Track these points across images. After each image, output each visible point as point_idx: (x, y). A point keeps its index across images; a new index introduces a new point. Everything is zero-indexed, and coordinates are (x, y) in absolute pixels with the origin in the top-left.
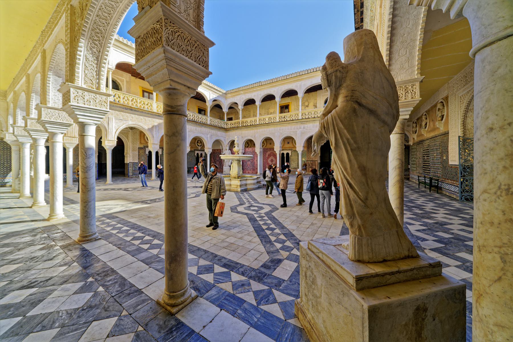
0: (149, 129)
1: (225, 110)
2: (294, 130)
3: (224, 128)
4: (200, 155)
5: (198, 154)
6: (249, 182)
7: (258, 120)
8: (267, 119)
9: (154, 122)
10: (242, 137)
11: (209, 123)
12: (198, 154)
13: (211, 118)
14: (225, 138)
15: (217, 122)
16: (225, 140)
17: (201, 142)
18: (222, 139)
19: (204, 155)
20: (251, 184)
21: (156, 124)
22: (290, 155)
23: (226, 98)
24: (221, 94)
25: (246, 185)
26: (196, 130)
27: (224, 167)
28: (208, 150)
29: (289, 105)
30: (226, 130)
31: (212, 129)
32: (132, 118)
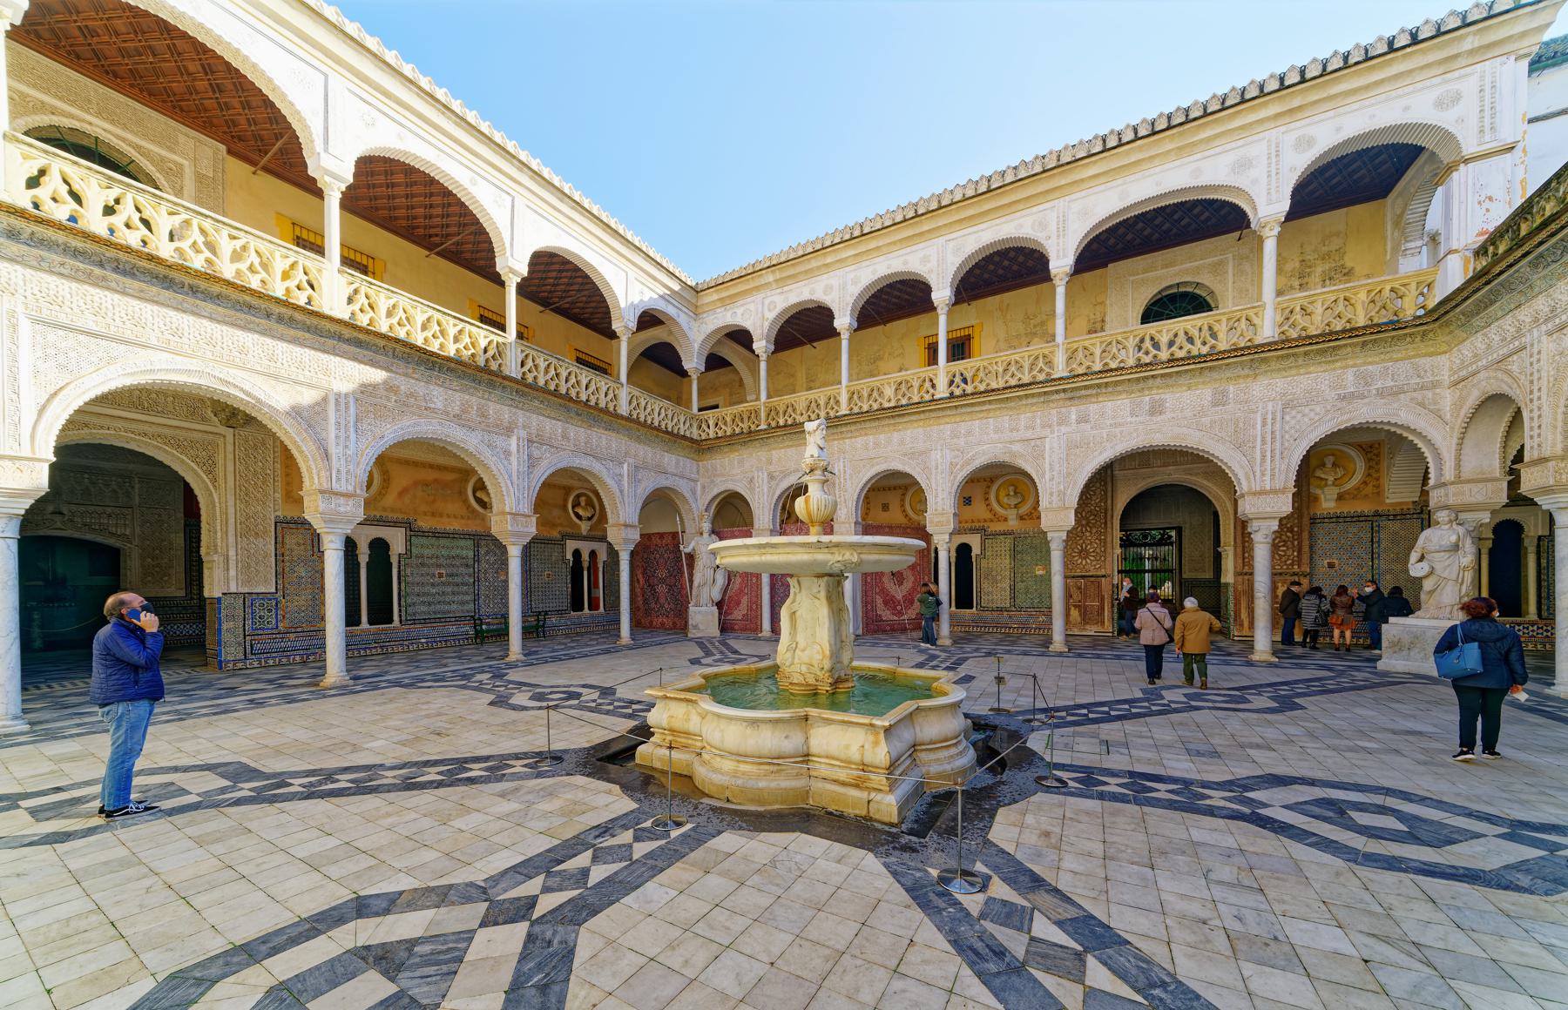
0: (296, 412)
2: (1029, 434)
3: (692, 440)
4: (585, 557)
5: (577, 554)
7: (844, 399)
8: (889, 391)
9: (326, 372)
10: (771, 477)
11: (624, 409)
12: (577, 554)
13: (636, 392)
14: (700, 483)
15: (656, 409)
16: (694, 492)
17: (590, 504)
18: (683, 486)
19: (602, 556)
21: (345, 387)
22: (976, 550)
26: (565, 436)
27: (692, 609)
28: (623, 531)
29: (969, 338)
30: (700, 448)
31: (639, 440)
32: (178, 332)
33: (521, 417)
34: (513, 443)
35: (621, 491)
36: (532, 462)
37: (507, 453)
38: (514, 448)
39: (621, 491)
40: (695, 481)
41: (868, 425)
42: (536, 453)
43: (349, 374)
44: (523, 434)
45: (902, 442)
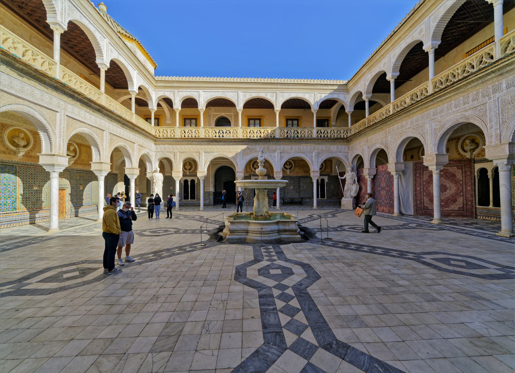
0: (233, 157)
1: (349, 109)
3: (344, 139)
6: (251, 228)
10: (368, 147)
11: (315, 135)
16: (347, 157)
18: (341, 156)
20: (254, 232)
21: (239, 151)
23: (347, 91)
24: (336, 87)
25: (247, 232)
27: (343, 198)
30: (347, 140)
31: (319, 144)
32: (218, 149)
33: (278, 147)
34: (276, 154)
35: (312, 161)
36: (281, 158)
37: (275, 157)
38: (276, 155)
39: (312, 161)
40: (348, 153)
41: (397, 119)
42: (283, 155)
43: (241, 147)
44: (279, 151)
45: (412, 123)
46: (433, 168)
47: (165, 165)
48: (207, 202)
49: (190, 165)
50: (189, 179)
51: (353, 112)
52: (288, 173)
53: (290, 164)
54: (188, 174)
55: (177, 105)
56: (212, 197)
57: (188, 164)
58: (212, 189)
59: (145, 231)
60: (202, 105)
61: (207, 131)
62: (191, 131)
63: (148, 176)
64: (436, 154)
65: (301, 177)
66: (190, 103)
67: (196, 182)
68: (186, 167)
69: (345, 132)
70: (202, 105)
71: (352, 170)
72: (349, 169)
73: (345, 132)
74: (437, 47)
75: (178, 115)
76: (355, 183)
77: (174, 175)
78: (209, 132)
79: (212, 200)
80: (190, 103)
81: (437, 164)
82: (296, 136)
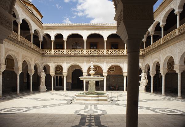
46: (178, 71)
47: (46, 69)
48: (68, 88)
49: (59, 69)
50: (59, 76)
51: (146, 41)
52: (112, 73)
53: (113, 68)
54: (58, 73)
55: (53, 38)
56: (70, 85)
57: (58, 68)
58: (70, 81)
59: (38, 99)
60: (65, 38)
61: (68, 51)
62: (59, 51)
63: (38, 74)
64: (179, 65)
65: (118, 75)
66: (59, 37)
67: (62, 77)
68: (57, 69)
69: (142, 52)
70: (65, 38)
71: (145, 72)
72: (143, 71)
73: (142, 52)
74: (181, 12)
75: (53, 43)
76: (145, 79)
77: (51, 74)
78: (69, 52)
79: (70, 87)
80: (59, 37)
81: (179, 70)
82: (115, 53)
